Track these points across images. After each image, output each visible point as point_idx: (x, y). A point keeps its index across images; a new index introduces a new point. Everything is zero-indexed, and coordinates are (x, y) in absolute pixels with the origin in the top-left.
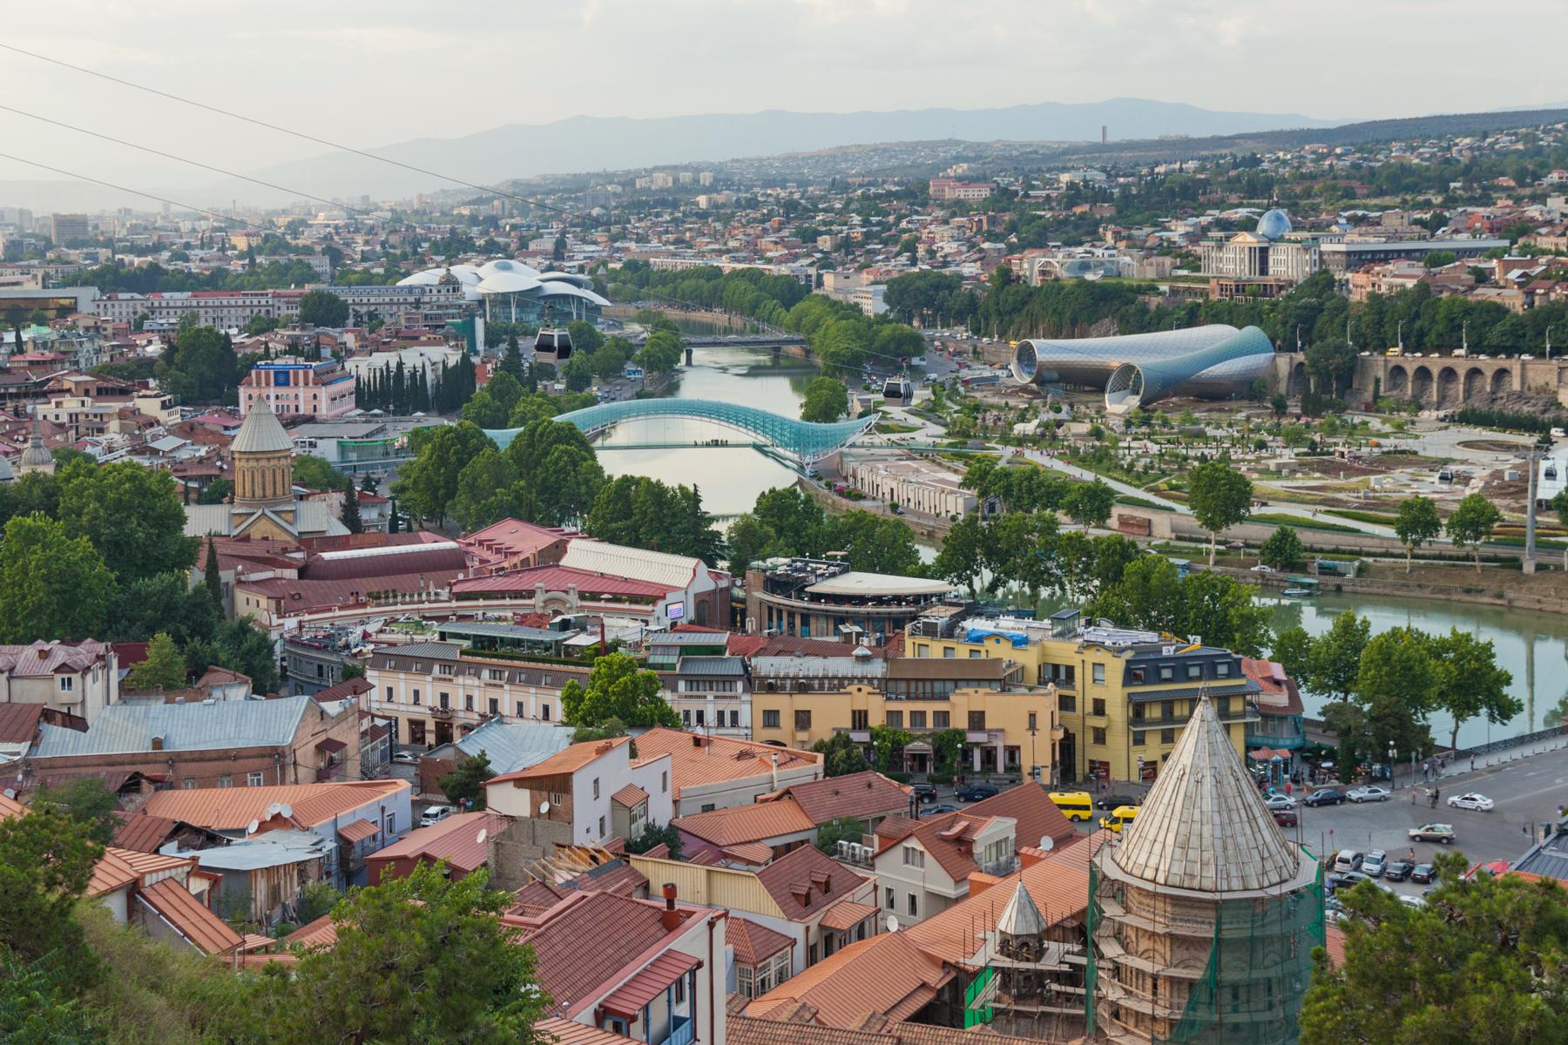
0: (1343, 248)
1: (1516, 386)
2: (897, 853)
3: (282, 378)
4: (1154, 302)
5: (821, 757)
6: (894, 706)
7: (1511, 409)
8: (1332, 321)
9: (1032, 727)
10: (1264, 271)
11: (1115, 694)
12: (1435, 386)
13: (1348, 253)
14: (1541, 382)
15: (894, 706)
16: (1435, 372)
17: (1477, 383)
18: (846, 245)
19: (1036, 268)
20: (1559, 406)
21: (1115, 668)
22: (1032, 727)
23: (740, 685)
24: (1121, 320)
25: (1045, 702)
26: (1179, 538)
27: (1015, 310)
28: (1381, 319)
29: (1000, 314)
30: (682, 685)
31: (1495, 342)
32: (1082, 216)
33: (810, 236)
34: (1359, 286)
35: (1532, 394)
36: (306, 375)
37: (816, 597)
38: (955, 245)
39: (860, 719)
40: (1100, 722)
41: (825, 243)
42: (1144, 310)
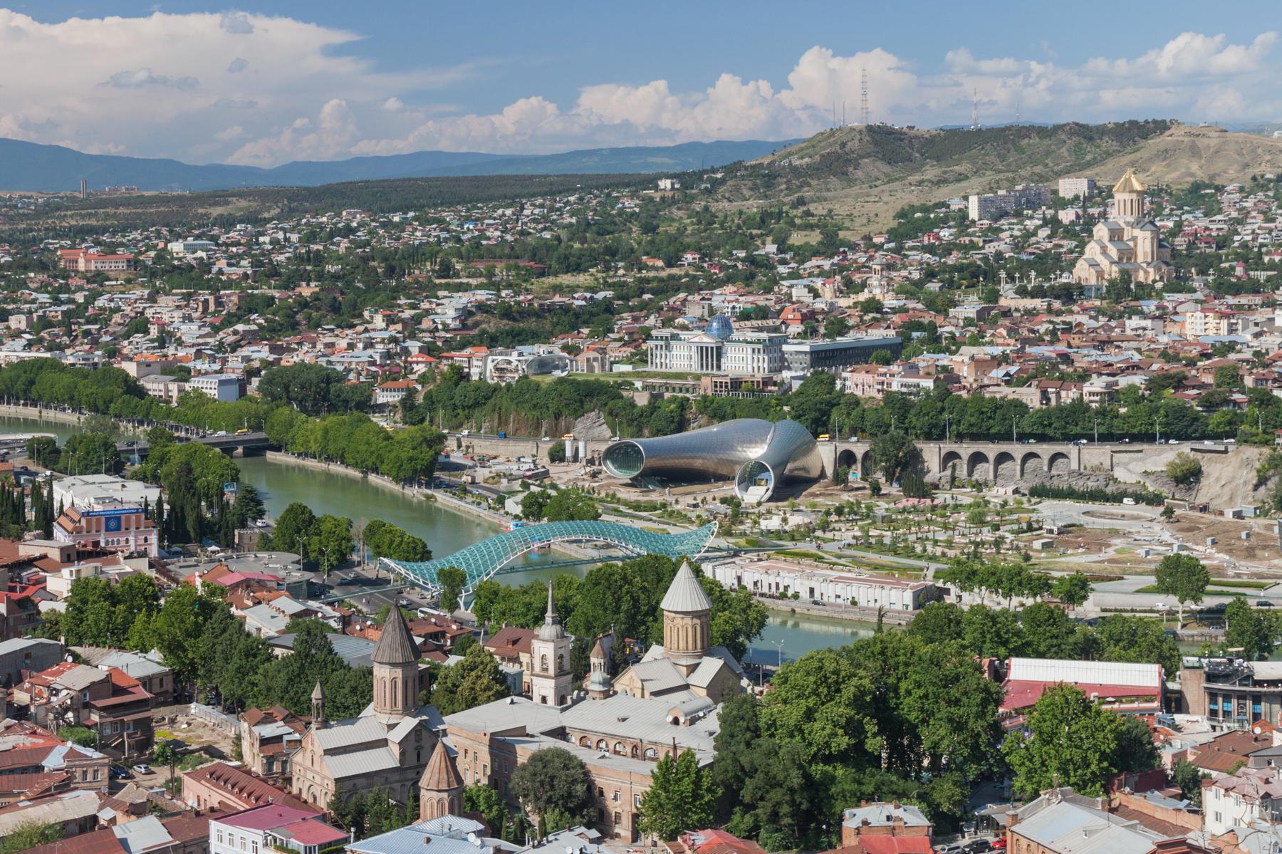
0: (807, 348)
1: (1074, 466)
3: (113, 524)
4: (642, 400)
7: (1079, 485)
8: (849, 414)
10: (719, 367)
12: (992, 467)
13: (812, 353)
14: (1096, 462)
16: (991, 457)
17: (1031, 463)
18: (46, 323)
19: (490, 366)
20: (1116, 480)
24: (610, 413)
26: (1104, 610)
27: (477, 404)
28: (907, 411)
29: (455, 407)
31: (1028, 430)
32: (316, 297)
34: (859, 383)
35: (1088, 472)
36: (138, 520)
38: (194, 327)
42: (632, 405)
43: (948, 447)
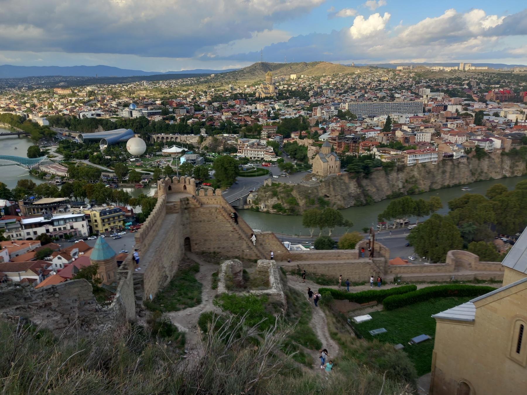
2: (56, 258)
5: (39, 241)
6: (54, 227)
9: (83, 226)
10: (132, 116)
11: (98, 218)
15: (54, 227)
21: (98, 214)
22: (83, 226)
23: (20, 229)
25: (85, 223)
30: (7, 231)
33: (25, 103)
37: (36, 205)
39: (48, 231)
40: (96, 224)
41: (28, 105)
43: (157, 136)
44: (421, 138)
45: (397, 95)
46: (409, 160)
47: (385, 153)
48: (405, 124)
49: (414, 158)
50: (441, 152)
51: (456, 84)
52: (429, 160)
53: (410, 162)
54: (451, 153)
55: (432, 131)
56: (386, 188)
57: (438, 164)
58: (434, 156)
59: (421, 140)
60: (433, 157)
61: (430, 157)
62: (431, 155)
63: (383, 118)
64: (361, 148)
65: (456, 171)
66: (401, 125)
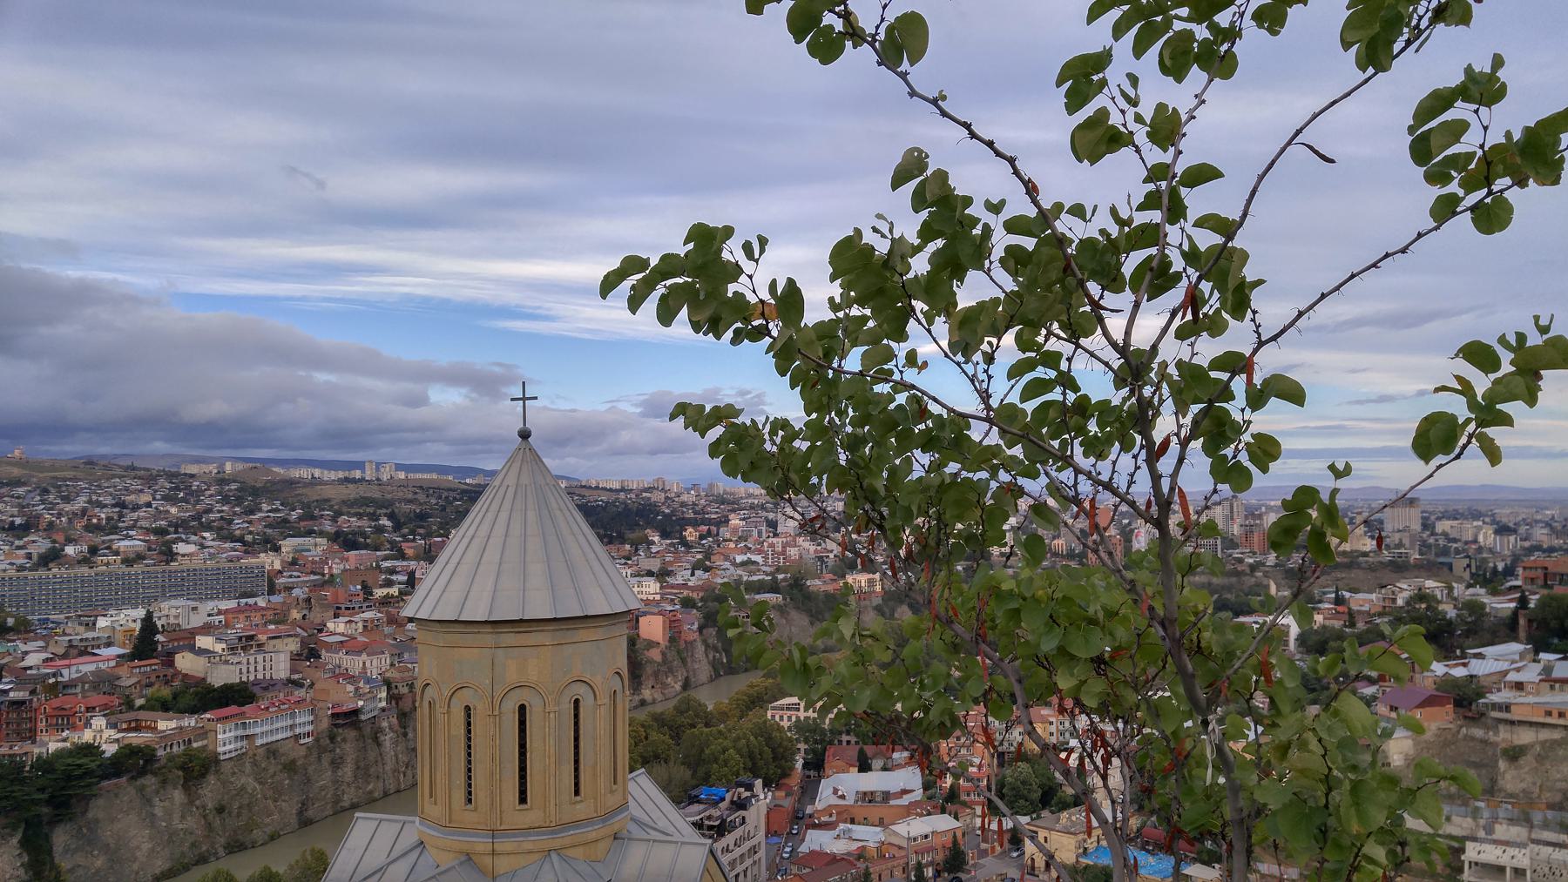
44: (260, 668)
45: (181, 548)
46: (225, 739)
47: (137, 729)
48: (206, 629)
49: (240, 732)
50: (320, 705)
51: (360, 516)
52: (289, 734)
53: (228, 747)
54: (351, 706)
55: (293, 645)
56: (146, 846)
57: (317, 740)
58: (303, 720)
59: (260, 676)
60: (298, 721)
61: (290, 722)
62: (293, 716)
63: (131, 618)
64: (42, 725)
65: (372, 755)
66: (193, 633)
